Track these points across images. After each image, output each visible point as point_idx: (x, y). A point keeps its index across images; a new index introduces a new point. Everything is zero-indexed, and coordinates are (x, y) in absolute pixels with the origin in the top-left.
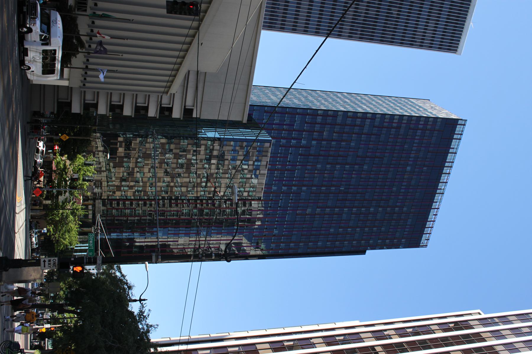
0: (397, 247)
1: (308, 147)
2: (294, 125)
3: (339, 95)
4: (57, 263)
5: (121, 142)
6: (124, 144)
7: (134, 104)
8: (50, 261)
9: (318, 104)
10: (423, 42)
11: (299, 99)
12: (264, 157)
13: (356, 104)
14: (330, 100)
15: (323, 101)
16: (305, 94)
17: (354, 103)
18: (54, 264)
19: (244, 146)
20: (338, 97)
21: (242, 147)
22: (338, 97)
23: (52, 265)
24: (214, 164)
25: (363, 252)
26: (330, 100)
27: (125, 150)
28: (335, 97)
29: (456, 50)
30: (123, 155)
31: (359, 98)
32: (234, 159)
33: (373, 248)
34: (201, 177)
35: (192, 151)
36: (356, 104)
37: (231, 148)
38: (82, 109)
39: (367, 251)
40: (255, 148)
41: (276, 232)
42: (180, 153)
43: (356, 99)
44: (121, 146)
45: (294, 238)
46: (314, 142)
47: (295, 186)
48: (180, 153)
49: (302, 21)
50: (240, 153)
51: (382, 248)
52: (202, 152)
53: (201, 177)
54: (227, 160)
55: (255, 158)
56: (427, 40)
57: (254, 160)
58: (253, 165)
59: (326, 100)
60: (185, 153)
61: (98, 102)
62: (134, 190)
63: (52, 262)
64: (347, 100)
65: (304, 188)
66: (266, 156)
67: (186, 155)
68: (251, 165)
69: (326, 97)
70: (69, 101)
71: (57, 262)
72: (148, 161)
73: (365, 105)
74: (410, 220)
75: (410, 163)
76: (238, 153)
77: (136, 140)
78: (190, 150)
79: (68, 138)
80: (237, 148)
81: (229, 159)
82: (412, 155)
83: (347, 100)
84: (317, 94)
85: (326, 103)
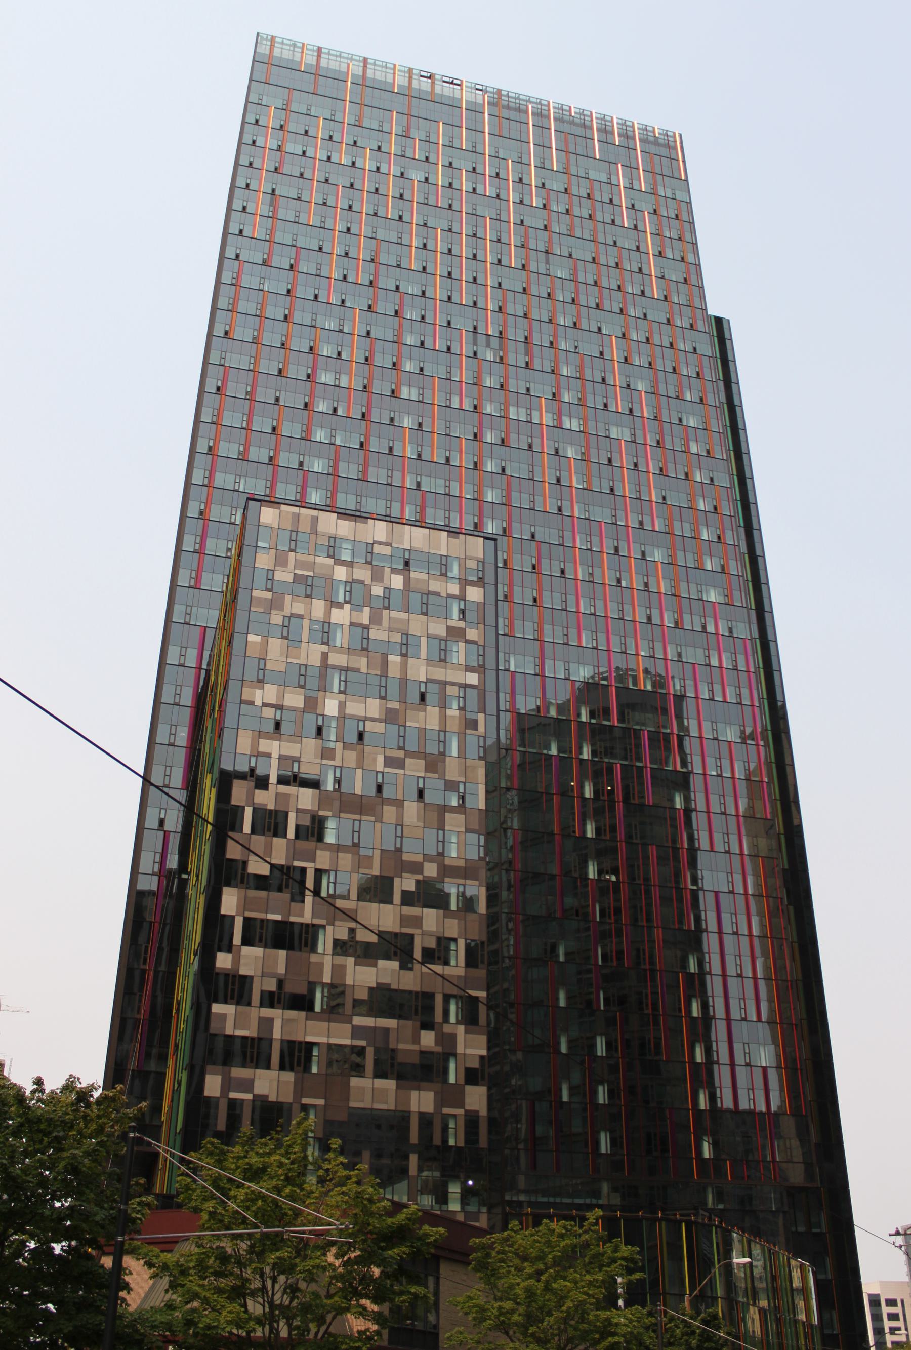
1: (336, 454)
5: (227, 1085)
6: (238, 1072)
12: (320, 528)
19: (269, 595)
21: (275, 604)
24: (342, 706)
32: (325, 633)
34: (401, 754)
35: (283, 789)
37: (276, 645)
40: (280, 560)
41: (658, 555)
42: (291, 833)
44: (247, 1085)
46: (319, 435)
50: (298, 608)
52: (292, 749)
53: (401, 754)
54: (325, 656)
55: (322, 560)
58: (350, 564)
60: (292, 817)
62: (461, 1029)
67: (298, 811)
72: (321, 965)
74: (593, 175)
76: (301, 617)
77: (224, 1016)
80: (277, 618)
81: (325, 648)
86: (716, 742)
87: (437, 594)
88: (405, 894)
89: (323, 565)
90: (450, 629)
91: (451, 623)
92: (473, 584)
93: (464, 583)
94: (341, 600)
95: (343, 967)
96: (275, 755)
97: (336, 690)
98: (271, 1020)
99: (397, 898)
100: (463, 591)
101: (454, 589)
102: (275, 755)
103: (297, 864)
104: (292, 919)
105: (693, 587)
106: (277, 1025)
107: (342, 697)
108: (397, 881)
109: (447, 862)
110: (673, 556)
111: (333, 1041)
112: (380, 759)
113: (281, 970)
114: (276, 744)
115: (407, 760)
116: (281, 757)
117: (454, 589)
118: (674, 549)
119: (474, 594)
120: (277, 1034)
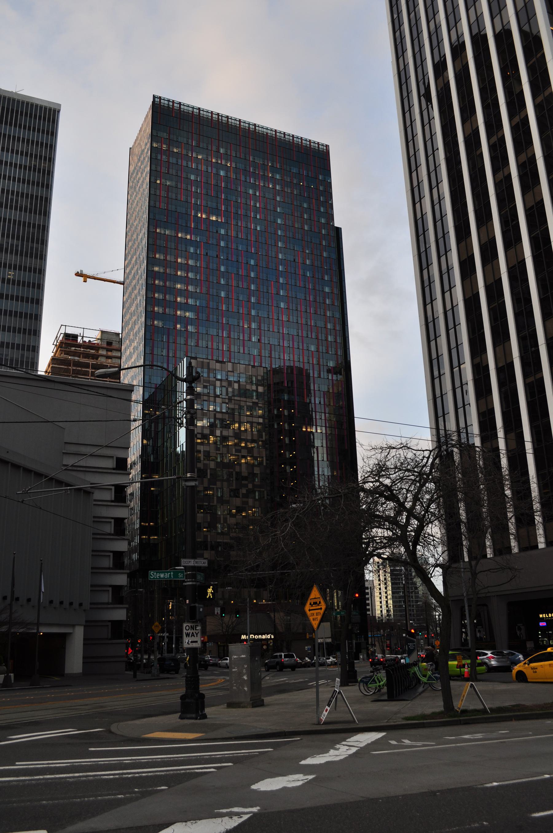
0: (328, 186)
2: (169, 329)
3: (127, 271)
4: (192, 625)
7: (112, 537)
8: (188, 635)
9: (139, 298)
10: (45, 158)
11: (135, 323)
13: (138, 247)
14: (134, 282)
15: (136, 292)
16: (127, 317)
17: (136, 250)
18: (192, 628)
20: (130, 272)
22: (130, 272)
23: (194, 631)
24: (221, 432)
25: (338, 231)
26: (134, 282)
27: (207, 549)
28: (130, 277)
29: (55, 111)
30: (213, 552)
31: (130, 244)
33: (330, 217)
34: (239, 448)
35: (206, 462)
36: (138, 247)
38: (121, 606)
39: (336, 224)
41: (313, 348)
42: (209, 477)
43: (131, 247)
45: (321, 324)
47: (250, 324)
48: (209, 477)
49: (23, 323)
51: (331, 206)
56: (41, 151)
57: (215, 379)
59: (134, 288)
60: (209, 471)
61: (110, 586)
63: (190, 631)
64: (134, 260)
65: (253, 313)
66: (209, 363)
67: (211, 469)
68: (221, 384)
69: (130, 288)
70: (110, 624)
71: (190, 625)
72: (220, 518)
73: (138, 235)
75: (214, 171)
78: (204, 464)
79: (157, 623)
82: (204, 168)
83: (134, 260)
84: (127, 300)
85: (138, 287)
86: (321, 385)
87: (249, 390)
88: (243, 494)
89: (213, 381)
90: (253, 403)
91: (253, 401)
92: (260, 385)
93: (257, 385)
94: (219, 394)
95: (226, 518)
96: (202, 450)
97: (219, 426)
98: (207, 536)
99: (241, 496)
100: (257, 388)
101: (254, 388)
102: (202, 450)
103: (211, 486)
104: (211, 504)
105: (325, 361)
106: (209, 536)
107: (221, 429)
108: (240, 490)
109: (255, 483)
110: (318, 348)
111: (225, 541)
112: (234, 450)
113: (209, 520)
114: (202, 446)
115: (242, 450)
116: (204, 451)
117: (254, 388)
118: (318, 345)
119: (261, 389)
120: (209, 540)
